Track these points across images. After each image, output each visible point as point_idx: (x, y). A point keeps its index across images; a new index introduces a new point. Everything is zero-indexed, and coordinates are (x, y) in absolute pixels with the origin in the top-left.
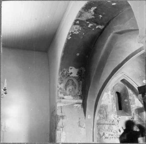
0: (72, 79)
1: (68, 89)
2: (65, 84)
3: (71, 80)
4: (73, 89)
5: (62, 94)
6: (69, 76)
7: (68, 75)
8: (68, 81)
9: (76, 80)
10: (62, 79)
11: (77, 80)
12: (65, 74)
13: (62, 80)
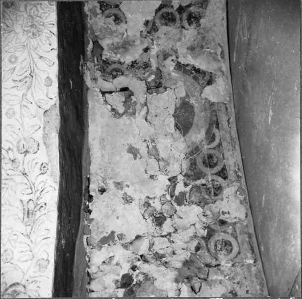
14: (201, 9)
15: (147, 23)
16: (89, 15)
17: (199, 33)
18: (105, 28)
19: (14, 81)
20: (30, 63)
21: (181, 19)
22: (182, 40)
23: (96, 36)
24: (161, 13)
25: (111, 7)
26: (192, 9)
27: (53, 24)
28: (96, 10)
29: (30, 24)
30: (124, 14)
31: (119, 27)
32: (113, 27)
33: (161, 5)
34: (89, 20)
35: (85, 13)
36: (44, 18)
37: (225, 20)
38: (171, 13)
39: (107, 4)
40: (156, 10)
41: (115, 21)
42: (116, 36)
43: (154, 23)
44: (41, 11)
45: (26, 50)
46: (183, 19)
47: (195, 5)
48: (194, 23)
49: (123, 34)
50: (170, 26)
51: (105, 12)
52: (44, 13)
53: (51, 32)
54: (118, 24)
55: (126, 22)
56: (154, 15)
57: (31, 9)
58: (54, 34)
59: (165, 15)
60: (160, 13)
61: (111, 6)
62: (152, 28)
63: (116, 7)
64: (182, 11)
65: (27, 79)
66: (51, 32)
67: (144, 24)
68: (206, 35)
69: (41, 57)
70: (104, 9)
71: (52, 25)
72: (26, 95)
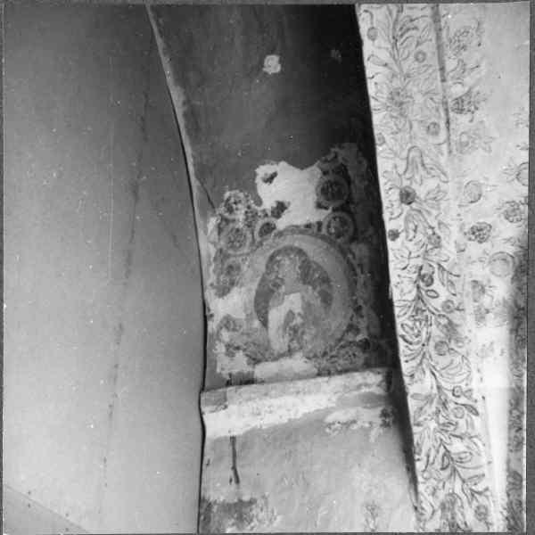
0: (296, 244)
1: (276, 316)
2: (254, 286)
3: (287, 251)
4: (308, 306)
5: (240, 355)
6: (268, 229)
7: (260, 223)
9: (325, 245)
10: (232, 259)
11: (332, 243)
13: (231, 267)
19: (416, 28)
20: (398, 54)
27: (375, 110)
29: (404, 106)
36: (388, 116)
44: (392, 124)
45: (405, 71)
57: (404, 125)
65: (400, 33)
69: (386, 65)
72: (398, 11)
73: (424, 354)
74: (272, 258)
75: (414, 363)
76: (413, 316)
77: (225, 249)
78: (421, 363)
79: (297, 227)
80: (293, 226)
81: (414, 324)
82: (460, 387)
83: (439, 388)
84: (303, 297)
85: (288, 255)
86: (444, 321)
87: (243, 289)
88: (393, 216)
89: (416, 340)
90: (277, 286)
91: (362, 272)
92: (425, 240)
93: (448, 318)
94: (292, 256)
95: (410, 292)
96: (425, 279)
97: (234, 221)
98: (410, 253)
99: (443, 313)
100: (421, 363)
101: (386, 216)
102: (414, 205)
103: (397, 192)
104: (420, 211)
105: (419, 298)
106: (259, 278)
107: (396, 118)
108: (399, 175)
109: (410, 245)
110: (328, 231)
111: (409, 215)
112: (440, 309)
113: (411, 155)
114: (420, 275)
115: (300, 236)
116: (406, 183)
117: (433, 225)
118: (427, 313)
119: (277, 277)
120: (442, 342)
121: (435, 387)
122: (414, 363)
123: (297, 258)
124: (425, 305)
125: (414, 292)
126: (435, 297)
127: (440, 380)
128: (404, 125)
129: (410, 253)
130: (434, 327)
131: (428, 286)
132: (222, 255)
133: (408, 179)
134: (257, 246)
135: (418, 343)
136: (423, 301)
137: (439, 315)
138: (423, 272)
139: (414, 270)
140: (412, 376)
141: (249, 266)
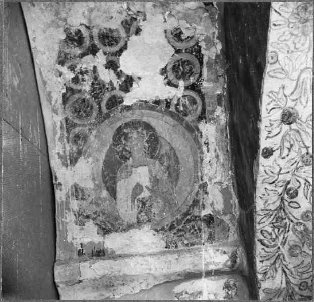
0: (145, 119)
1: (124, 188)
2: (102, 156)
3: (134, 125)
4: (155, 181)
5: (90, 224)
6: (114, 102)
7: (107, 96)
8: (120, 135)
10: (77, 130)
12: (88, 96)
13: (77, 137)
14: (67, 51)
15: (138, 31)
16: (215, 39)
17: (65, 20)
18: (195, 23)
21: (91, 37)
22: (88, 11)
23: (207, 11)
24: (119, 45)
25: (186, 50)
26: (78, 52)
27: (275, 25)
28: (206, 45)
30: (169, 42)
31: (176, 25)
32: (184, 25)
33: (120, 55)
34: (216, 33)
35: (221, 41)
36: (287, 33)
37: (31, 39)
38: (105, 45)
39: (191, 54)
40: (126, 49)
41: (181, 33)
42: (179, 12)
43: (128, 31)
44: (290, 43)
46: (88, 38)
47: (75, 56)
48: (74, 34)
49: (170, 15)
50: (106, 29)
51: (194, 44)
52: (285, 40)
53: (280, 14)
54: (177, 29)
55: (166, 31)
56: (129, 43)
58: (276, 11)
59: (114, 42)
60: (121, 44)
61: (186, 52)
62: (130, 25)
63: (179, 50)
64: (91, 48)
66: (280, 14)
67: (141, 30)
68: (54, 18)
70: (196, 47)
71: (276, 24)
73: (279, 255)
74: (119, 130)
75: (268, 263)
76: (272, 223)
77: (70, 118)
78: (274, 263)
79: (146, 102)
80: (142, 101)
81: (273, 230)
82: (307, 283)
83: (288, 282)
84: (150, 171)
85: (136, 129)
86: (302, 228)
87: (90, 159)
88: (270, 135)
89: (273, 243)
90: (125, 158)
91: (208, 151)
92: (298, 159)
93: (304, 226)
94: (140, 130)
95: (274, 203)
96: (291, 192)
97: (80, 91)
98: (281, 169)
99: (302, 221)
100: (274, 263)
101: (263, 135)
102: (294, 126)
103: (281, 111)
104: (298, 132)
105: (281, 208)
106: (107, 149)
107: (297, 36)
108: (286, 96)
109: (282, 162)
110: (177, 109)
111: (287, 134)
112: (299, 218)
113: (304, 76)
114: (286, 188)
115: (149, 111)
116: (290, 104)
117: (307, 145)
118: (287, 221)
119: (124, 149)
120: (296, 246)
121: (284, 282)
122: (268, 263)
123: (145, 132)
124: (286, 214)
125: (278, 204)
126: (297, 208)
127: (289, 277)
128: (303, 45)
129: (281, 169)
130: (291, 232)
131: (292, 197)
132: (69, 125)
133: (293, 100)
134: (103, 117)
135: (275, 245)
136: (284, 211)
137: (297, 224)
138: (289, 186)
139: (281, 184)
140: (265, 273)
141: (95, 136)
